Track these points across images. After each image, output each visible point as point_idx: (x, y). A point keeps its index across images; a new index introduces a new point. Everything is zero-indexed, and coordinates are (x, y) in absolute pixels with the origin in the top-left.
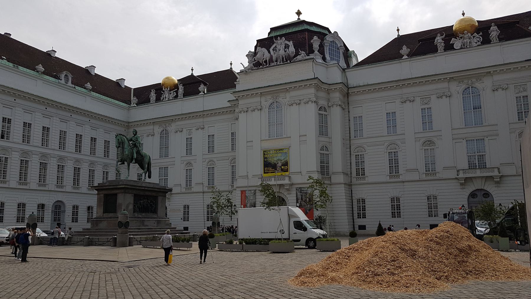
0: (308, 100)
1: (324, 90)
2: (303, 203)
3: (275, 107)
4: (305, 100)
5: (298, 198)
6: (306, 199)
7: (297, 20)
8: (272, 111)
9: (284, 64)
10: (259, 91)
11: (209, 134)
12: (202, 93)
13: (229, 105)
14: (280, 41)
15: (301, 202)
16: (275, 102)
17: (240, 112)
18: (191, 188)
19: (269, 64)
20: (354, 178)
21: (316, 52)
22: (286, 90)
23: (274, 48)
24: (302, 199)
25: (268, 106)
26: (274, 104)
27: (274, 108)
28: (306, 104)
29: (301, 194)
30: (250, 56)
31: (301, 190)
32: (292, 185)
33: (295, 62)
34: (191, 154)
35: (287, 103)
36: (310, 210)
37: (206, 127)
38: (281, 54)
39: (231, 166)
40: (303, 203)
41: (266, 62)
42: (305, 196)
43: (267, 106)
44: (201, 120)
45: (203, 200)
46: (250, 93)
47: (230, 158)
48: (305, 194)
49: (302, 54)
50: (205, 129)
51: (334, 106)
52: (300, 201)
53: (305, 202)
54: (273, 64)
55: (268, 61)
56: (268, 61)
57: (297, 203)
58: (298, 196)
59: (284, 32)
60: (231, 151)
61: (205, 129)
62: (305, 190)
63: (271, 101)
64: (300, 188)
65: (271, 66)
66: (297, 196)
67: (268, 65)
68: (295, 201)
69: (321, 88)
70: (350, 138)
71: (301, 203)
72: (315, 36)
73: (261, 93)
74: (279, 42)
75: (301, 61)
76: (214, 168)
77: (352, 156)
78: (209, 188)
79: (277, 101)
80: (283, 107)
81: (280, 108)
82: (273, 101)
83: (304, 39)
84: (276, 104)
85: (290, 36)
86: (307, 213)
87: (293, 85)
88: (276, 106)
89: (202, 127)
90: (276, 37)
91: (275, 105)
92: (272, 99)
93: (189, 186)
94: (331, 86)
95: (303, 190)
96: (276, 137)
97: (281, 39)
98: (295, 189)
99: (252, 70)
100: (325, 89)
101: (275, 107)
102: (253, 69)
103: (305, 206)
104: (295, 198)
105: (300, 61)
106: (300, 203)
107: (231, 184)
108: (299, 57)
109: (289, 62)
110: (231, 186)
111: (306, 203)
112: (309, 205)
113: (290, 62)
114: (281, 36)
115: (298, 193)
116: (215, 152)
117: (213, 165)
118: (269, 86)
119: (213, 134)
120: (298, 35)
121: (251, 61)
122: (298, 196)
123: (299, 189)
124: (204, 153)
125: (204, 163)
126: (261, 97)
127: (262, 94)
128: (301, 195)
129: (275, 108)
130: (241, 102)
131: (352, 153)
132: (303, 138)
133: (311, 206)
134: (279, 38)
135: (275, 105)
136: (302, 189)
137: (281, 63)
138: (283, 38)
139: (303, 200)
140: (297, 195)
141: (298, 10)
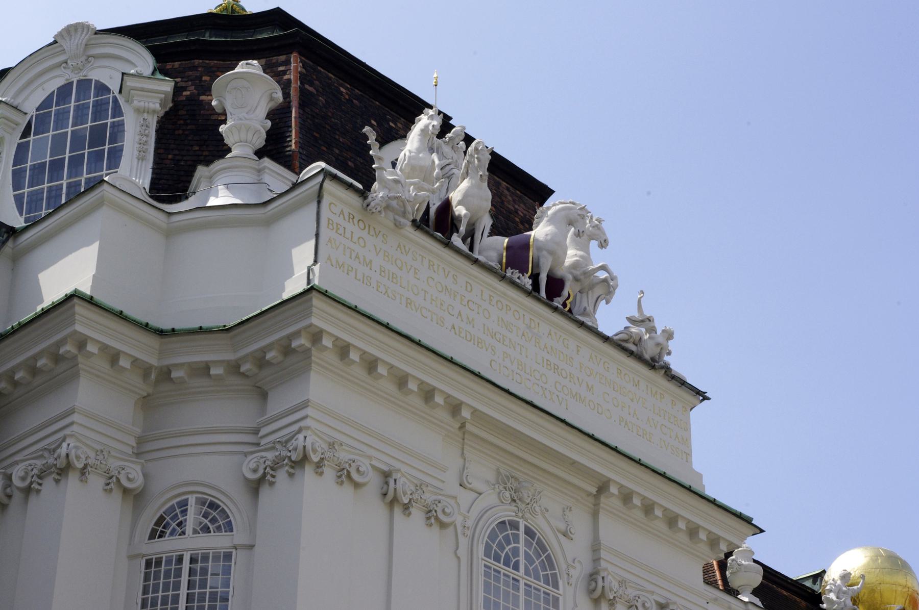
22: (594, 490)
27: (516, 567)
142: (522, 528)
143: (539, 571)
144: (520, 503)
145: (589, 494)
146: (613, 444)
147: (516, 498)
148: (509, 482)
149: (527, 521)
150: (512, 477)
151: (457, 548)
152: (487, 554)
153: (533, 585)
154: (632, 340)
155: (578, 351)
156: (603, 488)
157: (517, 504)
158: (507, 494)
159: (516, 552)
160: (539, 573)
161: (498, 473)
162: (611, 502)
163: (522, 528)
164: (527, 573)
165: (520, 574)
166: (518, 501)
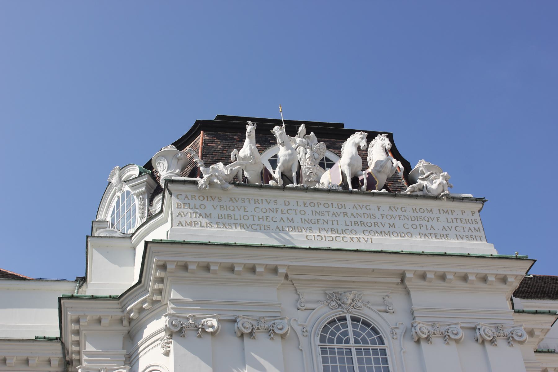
22: (399, 281)
26: (346, 326)
27: (347, 341)
33: (417, 197)
79: (356, 314)
80: (385, 341)
81: (373, 342)
91: (350, 329)
92: (334, 303)
135: (350, 329)
138: (312, 133)
142: (348, 318)
143: (366, 338)
144: (344, 305)
145: (397, 284)
146: (399, 250)
147: (340, 303)
148: (333, 296)
149: (351, 313)
150: (335, 293)
151: (299, 344)
152: (322, 340)
153: (363, 348)
154: (416, 190)
155: (379, 209)
157: (342, 306)
158: (334, 303)
159: (346, 333)
160: (358, 340)
161: (326, 294)
162: (412, 281)
163: (348, 318)
164: (357, 342)
165: (351, 344)
166: (342, 305)
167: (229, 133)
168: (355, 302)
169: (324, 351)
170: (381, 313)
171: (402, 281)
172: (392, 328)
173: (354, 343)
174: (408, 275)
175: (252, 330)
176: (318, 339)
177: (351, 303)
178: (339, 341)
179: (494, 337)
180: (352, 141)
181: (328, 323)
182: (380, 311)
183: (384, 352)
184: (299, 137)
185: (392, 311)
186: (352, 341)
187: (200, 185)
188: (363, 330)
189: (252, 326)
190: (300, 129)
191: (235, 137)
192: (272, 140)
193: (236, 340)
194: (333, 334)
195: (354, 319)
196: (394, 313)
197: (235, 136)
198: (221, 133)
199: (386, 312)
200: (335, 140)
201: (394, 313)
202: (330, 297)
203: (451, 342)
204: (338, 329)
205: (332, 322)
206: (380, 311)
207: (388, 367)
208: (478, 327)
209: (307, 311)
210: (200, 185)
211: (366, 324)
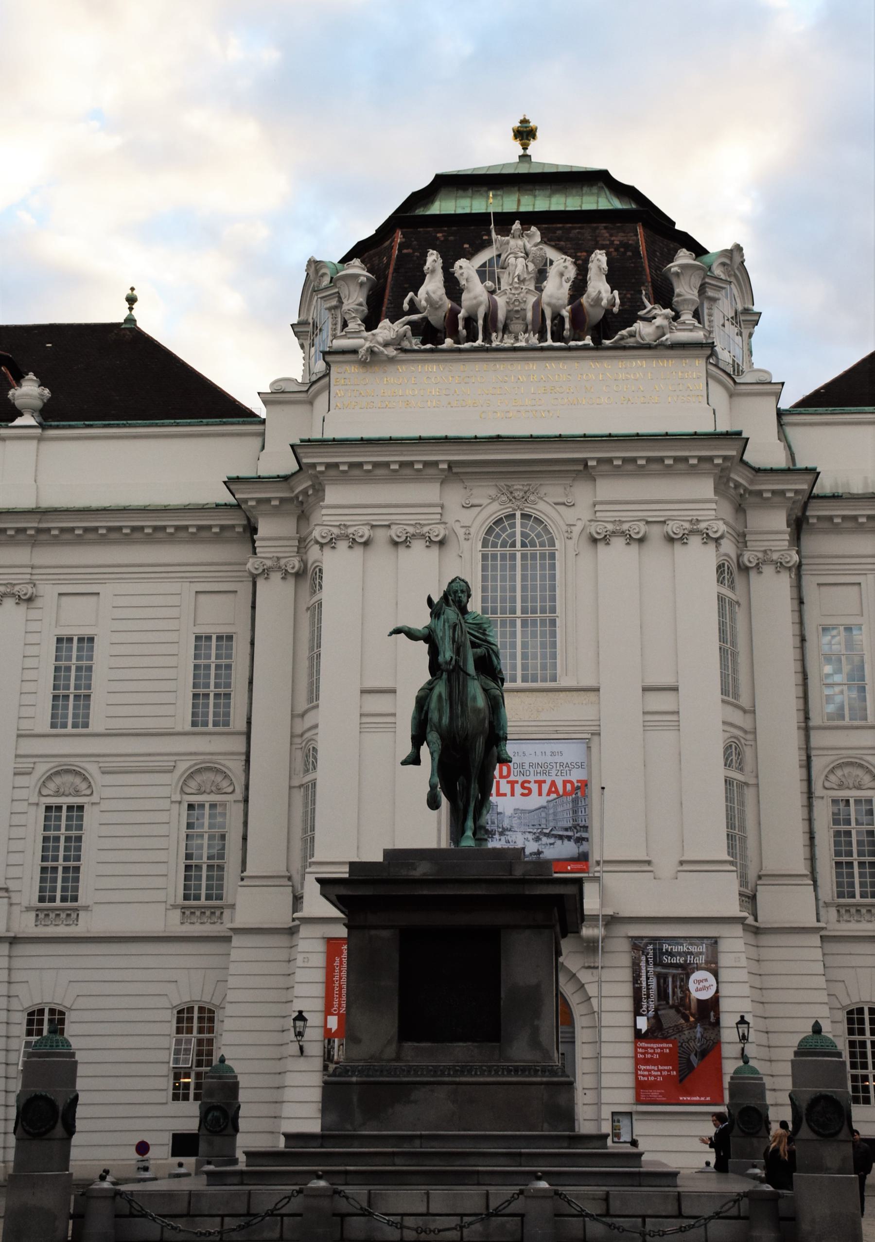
0: (687, 525)
1: (732, 492)
2: (670, 1017)
3: (518, 538)
4: (672, 527)
5: (644, 991)
6: (682, 999)
7: (518, 160)
8: (504, 557)
9: (570, 349)
10: (443, 456)
11: (65, 632)
12: (26, 420)
13: (226, 497)
14: (520, 242)
15: (656, 1010)
16: (518, 514)
17: (331, 543)
18: (76, 910)
19: (487, 338)
20: (827, 905)
21: (687, 317)
22: (581, 468)
23: (484, 265)
24: (662, 994)
25: (478, 531)
26: (513, 526)
27: (513, 545)
28: (678, 546)
29: (659, 969)
30: (362, 284)
31: (659, 953)
32: (612, 921)
33: (624, 348)
34: (86, 725)
35: (576, 530)
36: (703, 1054)
37: (48, 592)
38: (554, 301)
39: (185, 806)
40: (670, 1017)
41: (470, 321)
42: (682, 980)
43: (473, 530)
44: (20, 555)
45: (9, 983)
46: (394, 457)
47: (183, 766)
48: (680, 971)
49: (654, 318)
50: (39, 600)
51: (764, 567)
52: (652, 1006)
53: (678, 1011)
54: (508, 342)
55: (480, 322)
56: (480, 322)
57: (637, 1012)
58: (644, 978)
59: (559, 202)
60: (188, 727)
61: (38, 603)
62: (680, 954)
63: (494, 510)
64: (654, 940)
65: (498, 350)
66: (636, 979)
67: (479, 342)
68: (628, 1004)
69: (729, 479)
70: (807, 718)
71: (657, 1017)
72: (684, 250)
73: (450, 465)
74: (515, 243)
75: (655, 347)
76: (81, 808)
77: (816, 803)
78: (42, 914)
79: (528, 511)
80: (557, 542)
81: (542, 544)
82: (509, 511)
83: (629, 254)
84: (523, 525)
85: (560, 229)
86: (690, 1067)
87: (618, 453)
88: (523, 535)
89: (30, 590)
90: (504, 221)
91: (518, 529)
92: (504, 498)
93: (64, 899)
94: (762, 477)
95: (671, 954)
96: (519, 679)
97: (523, 229)
98: (624, 946)
99: (405, 351)
100: (737, 485)
101: (518, 538)
102: (406, 344)
103: (679, 1030)
104: (627, 989)
105: (648, 347)
106: (651, 1013)
107: (180, 900)
108: (643, 329)
109: (588, 340)
110: (178, 912)
111: (686, 1019)
112: (699, 1029)
113: (597, 341)
114: (529, 219)
115: (643, 964)
116: (97, 724)
117: (77, 793)
118: (499, 437)
119: (86, 632)
120: (597, 228)
121: (360, 305)
122: (644, 978)
123: (647, 945)
124: (26, 725)
125: (21, 781)
126: (442, 483)
127: (455, 470)
128: (659, 976)
129: (518, 544)
130: (334, 495)
131: (818, 790)
132: (661, 702)
133: (710, 1035)
134: (517, 226)
135: (518, 529)
136: (665, 947)
137: (549, 342)
139: (671, 1002)
140: (640, 976)
141: (524, 121)
149: (521, 510)
152: (485, 544)
156: (584, 462)
159: (513, 534)
167: (431, 229)
168: (528, 494)
169: (484, 557)
170: (557, 507)
171: (586, 465)
172: (567, 525)
173: (520, 546)
174: (590, 463)
175: (407, 537)
176: (480, 544)
177: (523, 497)
178: (504, 545)
179: (684, 534)
180: (556, 269)
181: (493, 524)
182: (556, 504)
183: (552, 556)
184: (514, 237)
185: (572, 504)
186: (518, 544)
187: (360, 357)
188: (532, 529)
189: (407, 533)
190: (514, 227)
191: (439, 235)
192: (486, 235)
193: (389, 549)
194: (498, 536)
195: (524, 516)
196: (574, 505)
197: (439, 232)
198: (421, 229)
199: (564, 504)
200: (570, 225)
201: (574, 505)
202: (501, 491)
203: (632, 542)
204: (504, 530)
205: (498, 522)
206: (556, 504)
207: (555, 574)
208: (667, 523)
209: (473, 508)
210: (360, 357)
211: (538, 521)
